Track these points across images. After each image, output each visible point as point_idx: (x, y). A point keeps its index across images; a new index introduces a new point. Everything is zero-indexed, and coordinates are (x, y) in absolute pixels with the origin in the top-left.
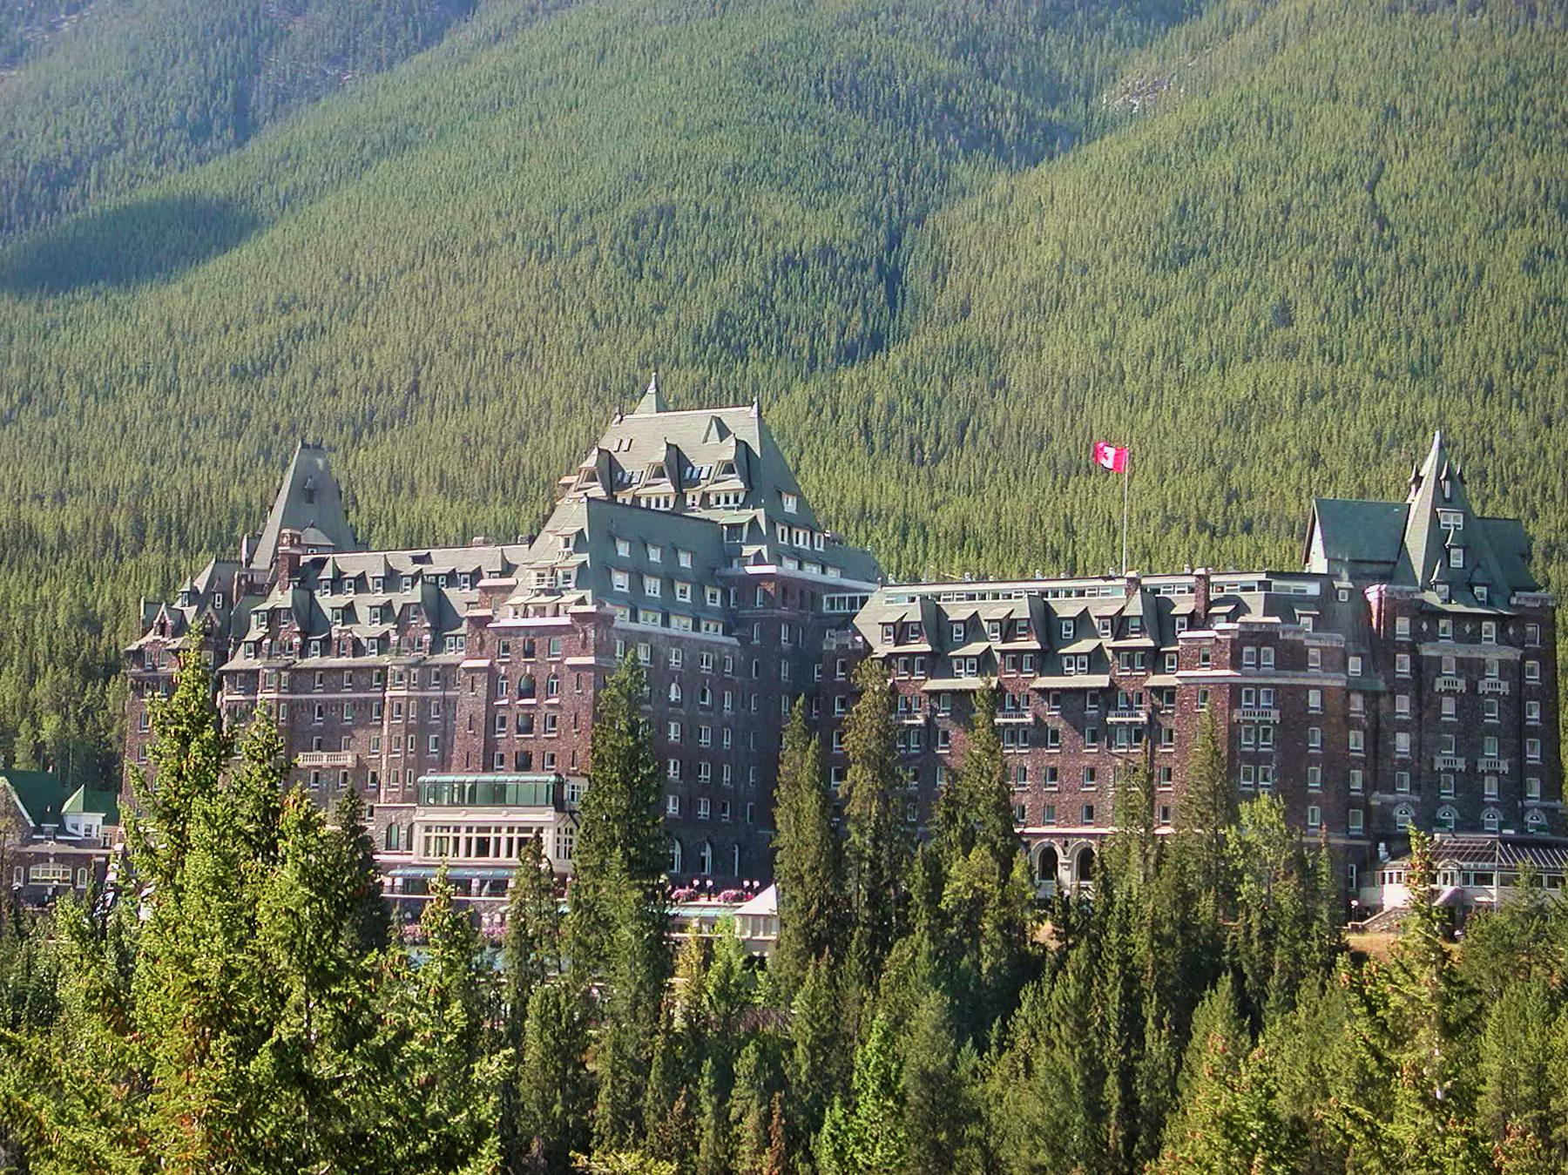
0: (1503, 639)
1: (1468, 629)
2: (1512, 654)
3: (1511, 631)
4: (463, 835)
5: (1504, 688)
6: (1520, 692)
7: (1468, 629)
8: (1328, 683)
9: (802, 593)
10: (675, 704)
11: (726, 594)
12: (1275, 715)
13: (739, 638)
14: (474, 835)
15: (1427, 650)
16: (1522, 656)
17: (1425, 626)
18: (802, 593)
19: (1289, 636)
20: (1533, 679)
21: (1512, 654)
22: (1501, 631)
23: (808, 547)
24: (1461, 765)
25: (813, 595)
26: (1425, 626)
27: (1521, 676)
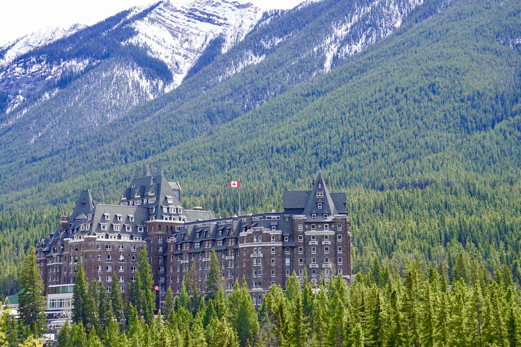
0: (331, 229)
1: (320, 226)
2: (332, 233)
3: (333, 226)
4: (57, 301)
5: (330, 243)
6: (336, 244)
7: (320, 226)
8: (277, 245)
9: (167, 226)
10: (123, 261)
11: (145, 229)
12: (261, 255)
13: (146, 241)
14: (59, 301)
15: (307, 233)
16: (335, 233)
17: (307, 227)
18: (167, 226)
19: (265, 232)
20: (339, 241)
21: (332, 233)
22: (330, 226)
23: (175, 213)
24: (317, 266)
25: (172, 227)
26: (307, 227)
27: (336, 240)
